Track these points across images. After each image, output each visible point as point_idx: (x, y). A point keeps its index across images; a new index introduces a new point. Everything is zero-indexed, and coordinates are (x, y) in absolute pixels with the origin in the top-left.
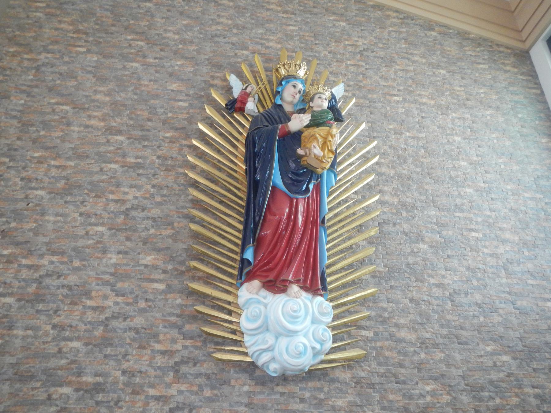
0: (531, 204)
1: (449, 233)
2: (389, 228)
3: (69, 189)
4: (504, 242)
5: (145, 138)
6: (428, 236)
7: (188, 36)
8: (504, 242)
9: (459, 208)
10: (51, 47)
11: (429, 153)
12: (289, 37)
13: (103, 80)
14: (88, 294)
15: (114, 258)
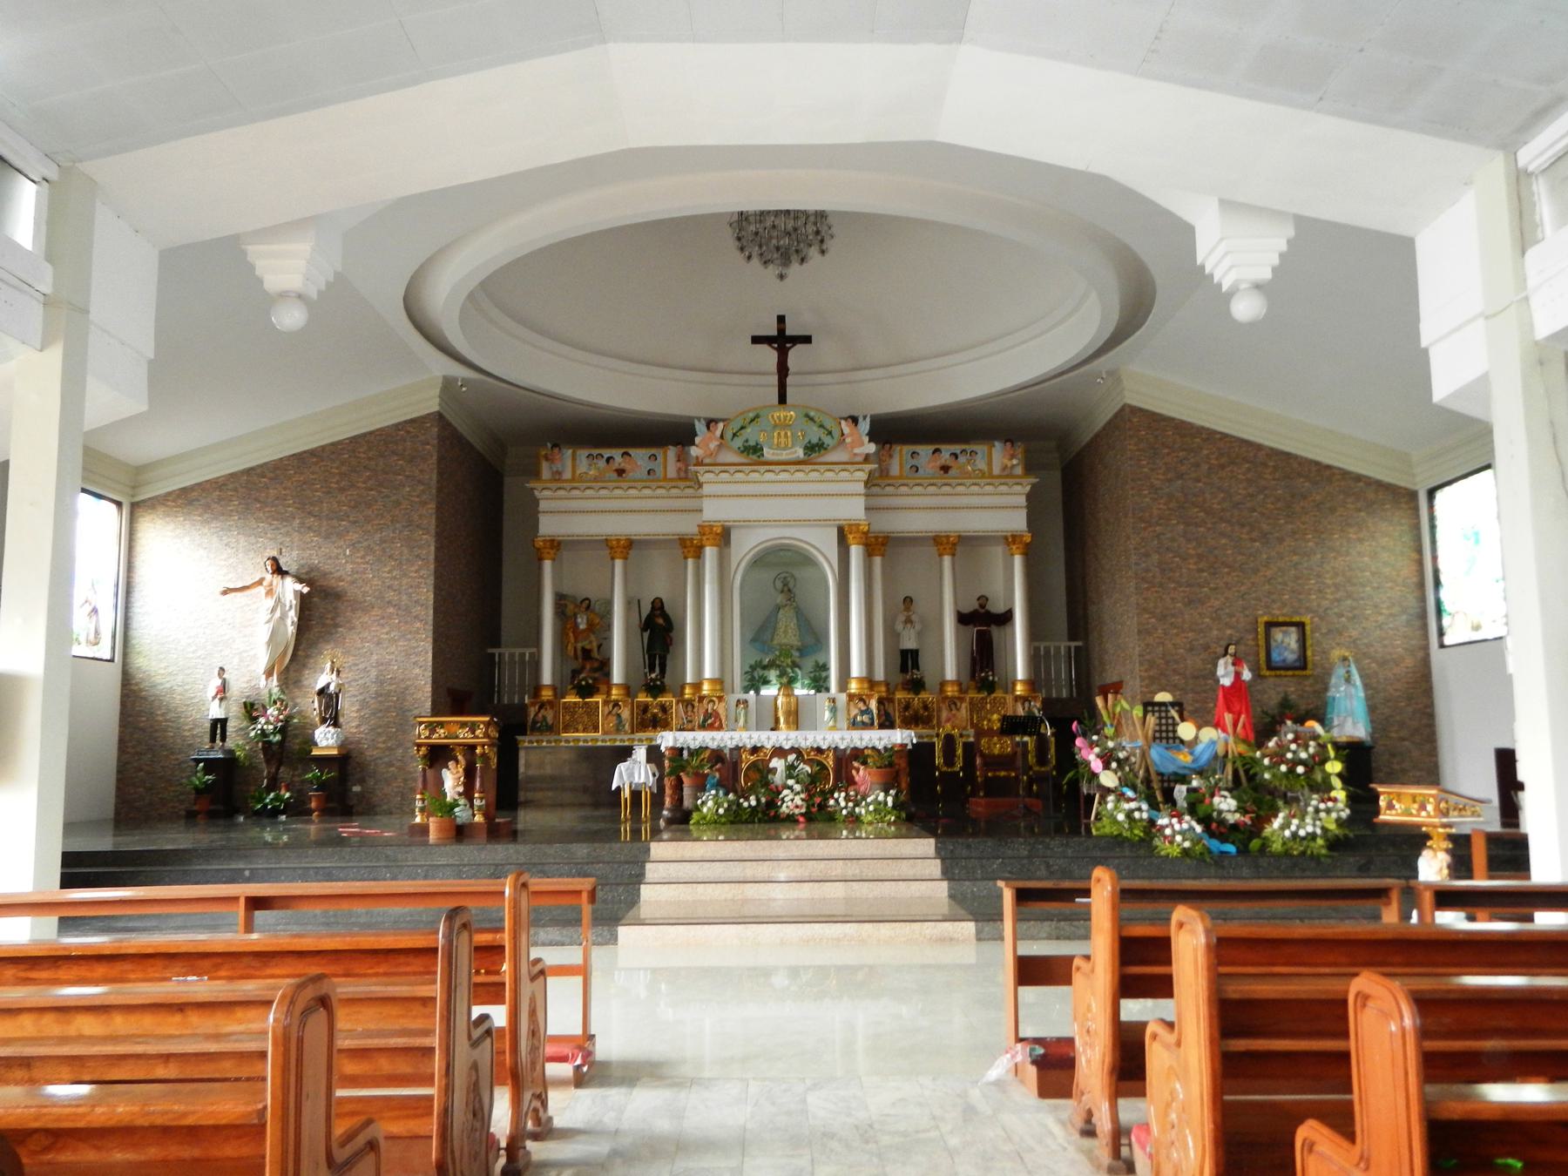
0: (1399, 593)
1: (1356, 612)
2: (1329, 612)
3: (1190, 602)
4: (1381, 614)
5: (1214, 574)
6: (1345, 613)
7: (1225, 505)
8: (1381, 614)
9: (1362, 599)
10: (1161, 521)
11: (1351, 569)
12: (1278, 500)
13: (1189, 541)
14: (1209, 647)
15: (1215, 632)
